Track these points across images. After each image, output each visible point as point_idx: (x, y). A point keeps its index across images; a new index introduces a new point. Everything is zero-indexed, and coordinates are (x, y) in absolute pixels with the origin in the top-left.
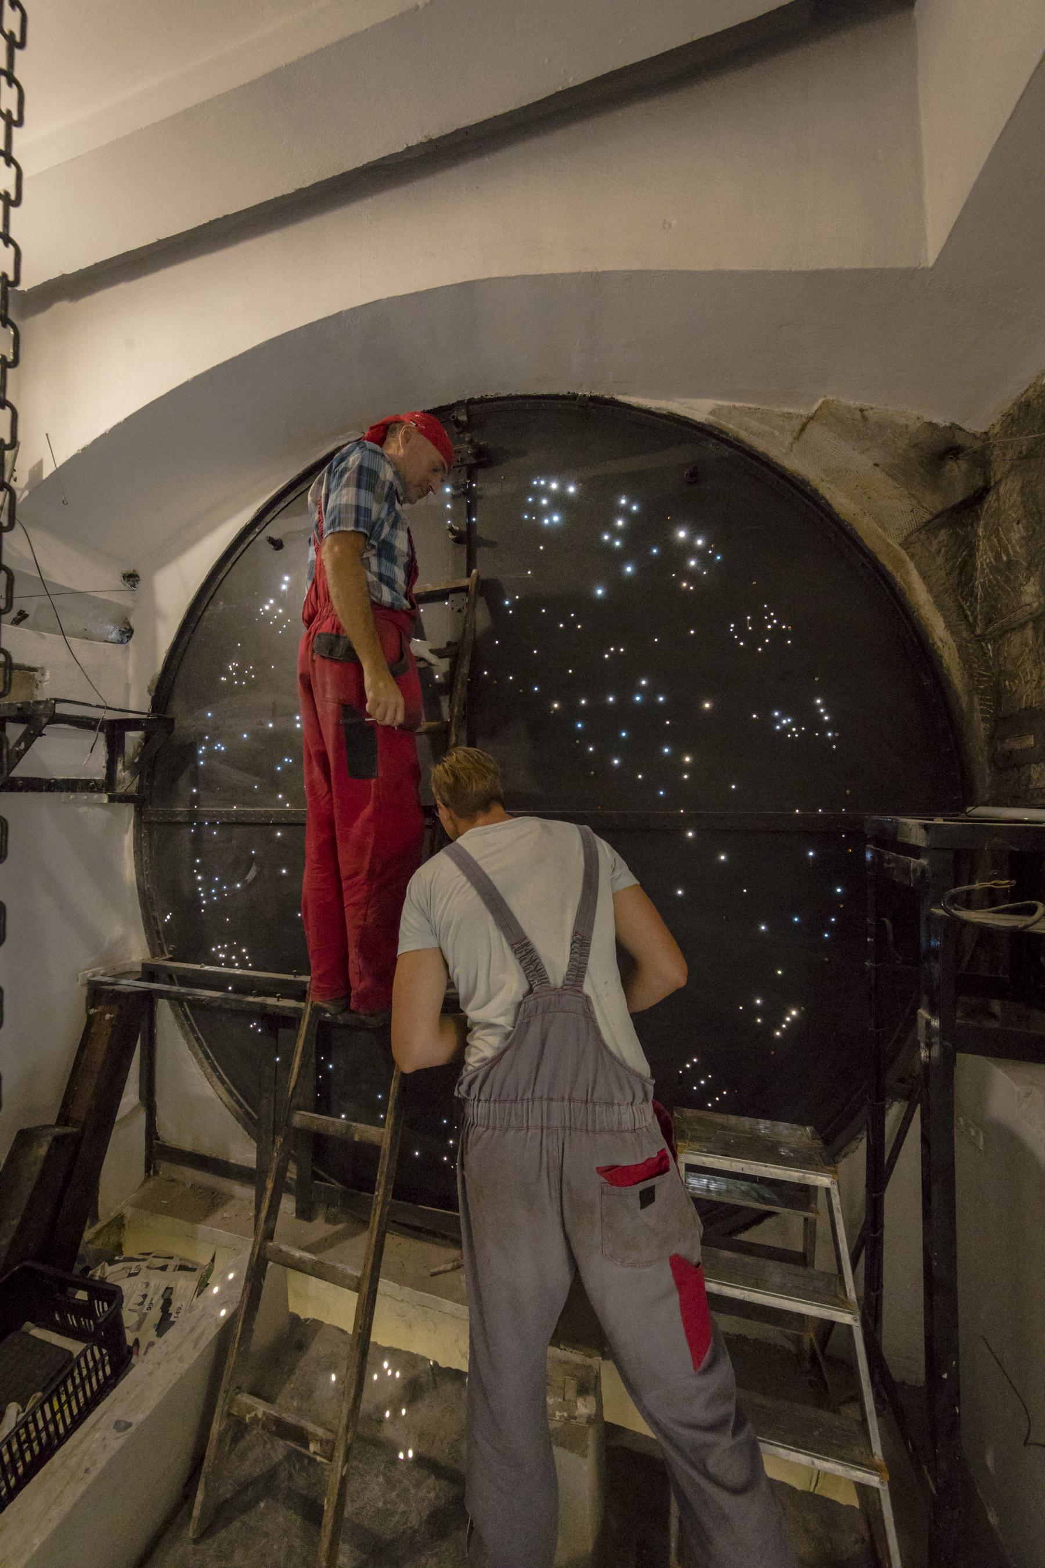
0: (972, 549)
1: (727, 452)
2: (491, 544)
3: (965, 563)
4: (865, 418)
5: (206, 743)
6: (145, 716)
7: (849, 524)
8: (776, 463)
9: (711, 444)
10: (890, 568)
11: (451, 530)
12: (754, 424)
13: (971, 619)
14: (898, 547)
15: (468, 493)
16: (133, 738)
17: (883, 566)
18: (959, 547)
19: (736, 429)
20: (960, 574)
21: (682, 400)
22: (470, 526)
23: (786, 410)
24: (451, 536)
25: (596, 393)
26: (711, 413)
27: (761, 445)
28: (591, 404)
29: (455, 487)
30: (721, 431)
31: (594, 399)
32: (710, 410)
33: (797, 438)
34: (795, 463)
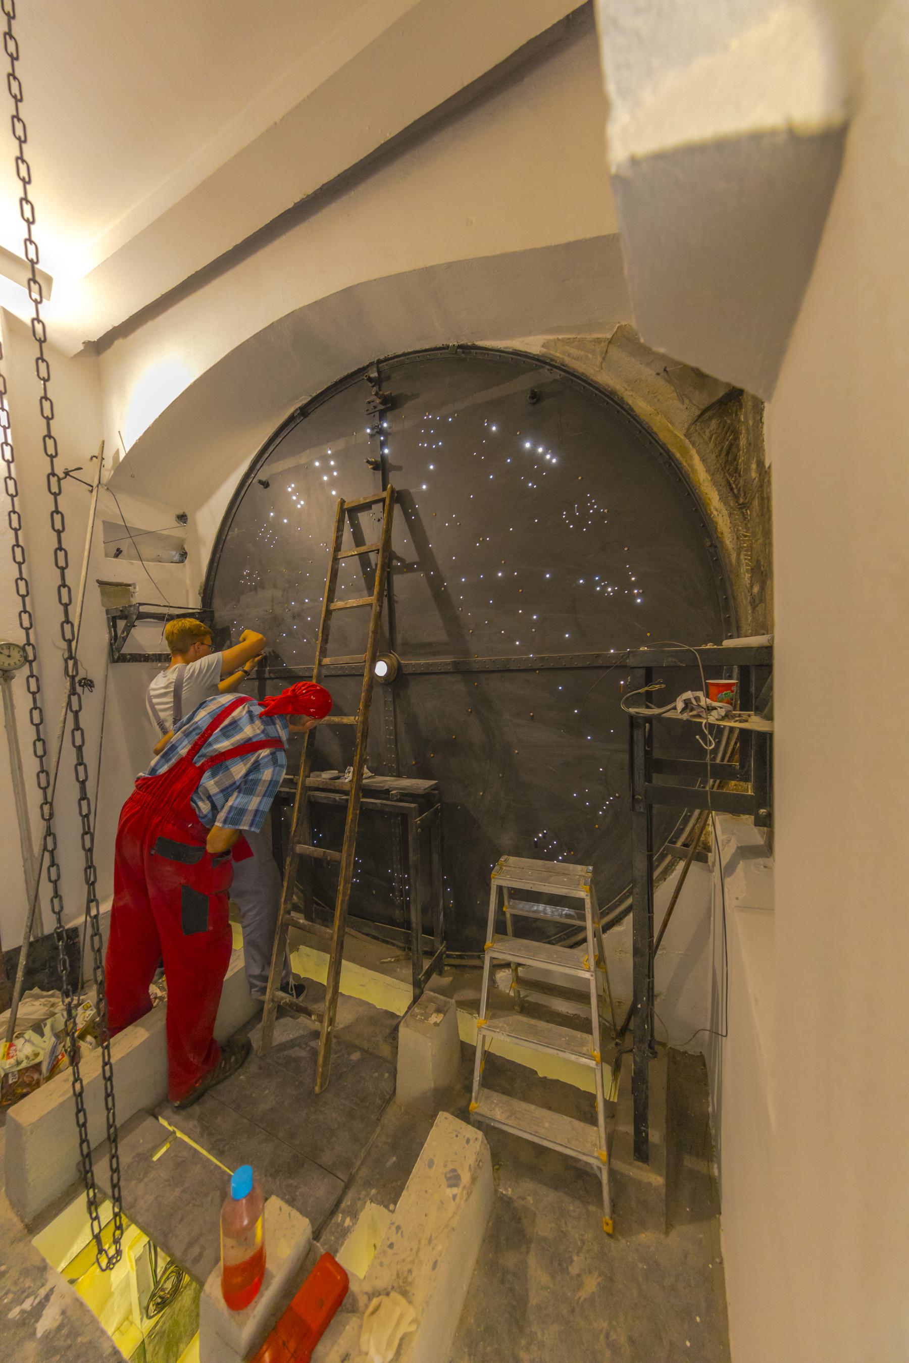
0: (736, 433)
2: (399, 468)
10: (678, 455)
14: (682, 437)
15: (381, 432)
17: (673, 454)
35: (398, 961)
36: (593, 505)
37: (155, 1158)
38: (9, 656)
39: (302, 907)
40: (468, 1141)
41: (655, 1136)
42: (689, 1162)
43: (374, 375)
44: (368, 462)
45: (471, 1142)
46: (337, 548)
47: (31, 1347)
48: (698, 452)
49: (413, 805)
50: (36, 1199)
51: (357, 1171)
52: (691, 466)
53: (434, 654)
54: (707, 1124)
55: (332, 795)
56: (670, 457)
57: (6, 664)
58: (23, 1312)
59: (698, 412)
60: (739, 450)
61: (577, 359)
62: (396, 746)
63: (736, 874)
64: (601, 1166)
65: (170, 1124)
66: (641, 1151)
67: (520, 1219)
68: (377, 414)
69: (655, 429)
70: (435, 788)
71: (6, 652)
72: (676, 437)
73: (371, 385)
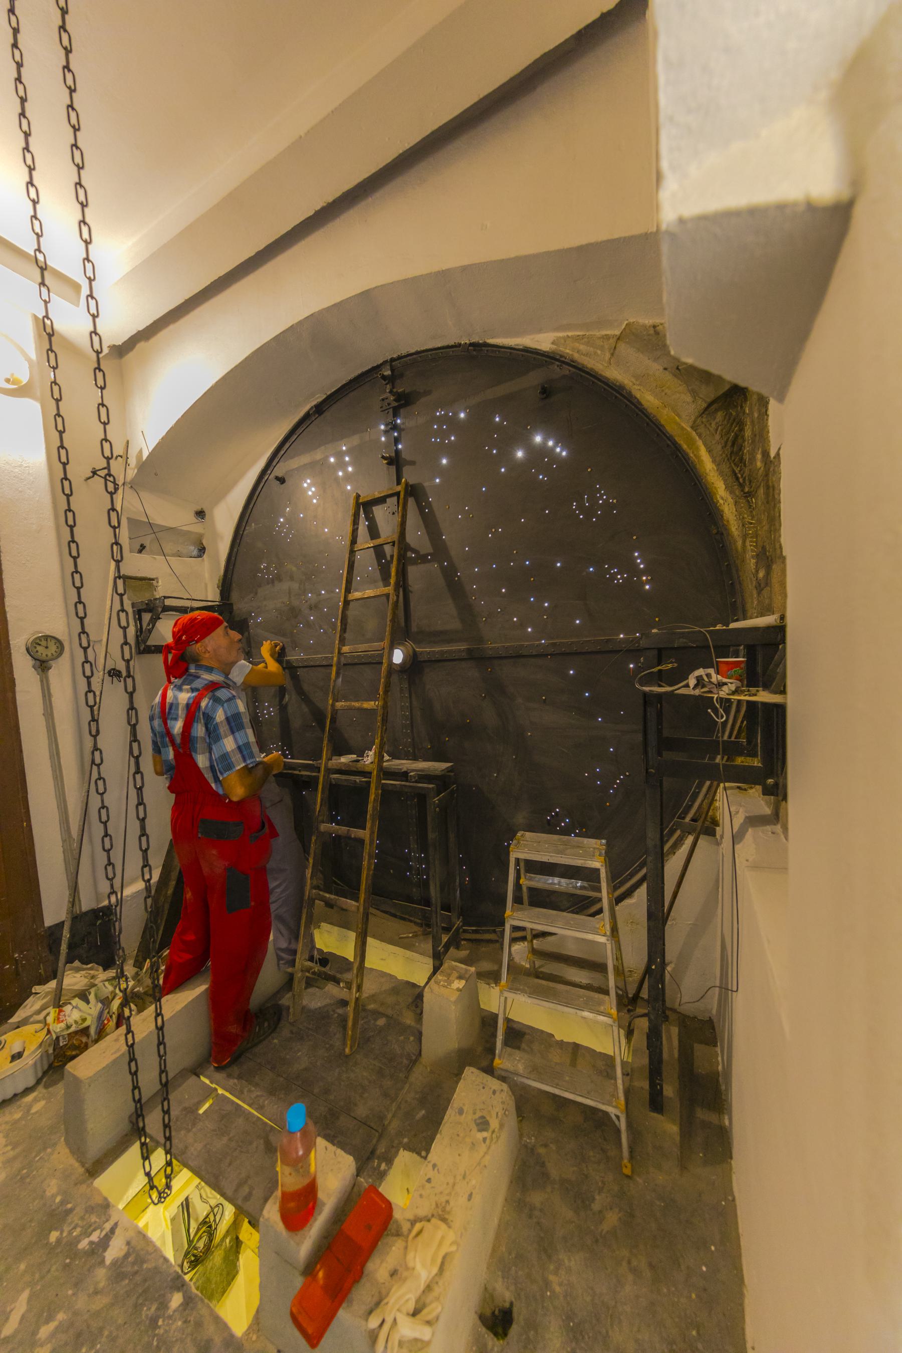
0: (741, 425)
2: (413, 463)
7: (654, 416)
8: (601, 375)
10: (685, 447)
14: (689, 429)
15: (395, 427)
20: (733, 445)
21: (532, 337)
23: (604, 332)
27: (590, 363)
29: (386, 425)
30: (561, 356)
32: (551, 341)
34: (614, 374)
35: (416, 936)
36: (602, 495)
37: (201, 1111)
38: (47, 647)
39: (322, 887)
40: (494, 1092)
41: (669, 1091)
42: (701, 1114)
43: (388, 373)
44: (383, 457)
45: (498, 1093)
46: (354, 541)
47: (101, 1274)
48: (705, 445)
49: (431, 786)
50: (95, 1146)
51: (390, 1123)
52: (698, 457)
53: (449, 641)
54: (718, 1081)
55: (352, 778)
56: (676, 448)
57: (44, 655)
58: (91, 1243)
59: (704, 405)
60: (744, 441)
61: (586, 355)
62: (412, 731)
63: (745, 840)
64: (619, 1114)
65: (211, 1083)
66: (656, 1103)
67: (543, 1163)
68: (391, 411)
69: (663, 422)
70: (449, 770)
71: (43, 643)
72: (683, 429)
73: (384, 383)
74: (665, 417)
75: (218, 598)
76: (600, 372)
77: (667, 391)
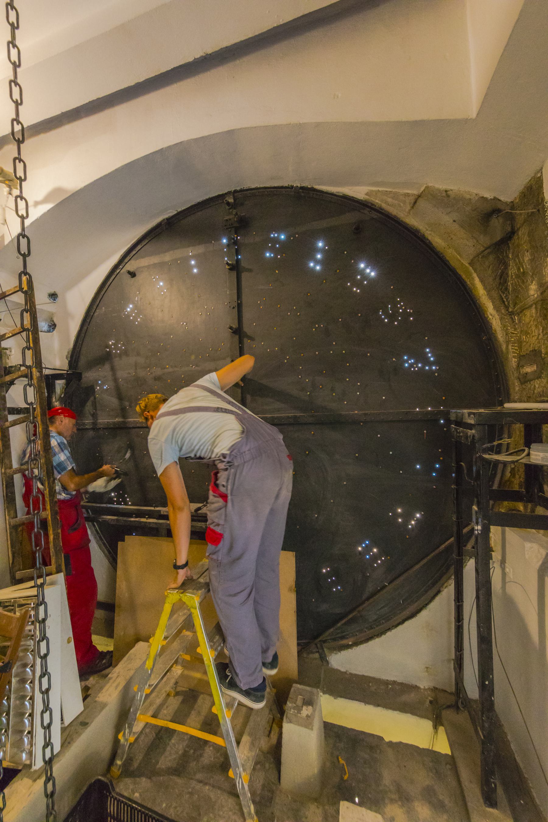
0: (506, 266)
1: (375, 215)
3: (502, 273)
4: (448, 196)
5: (99, 385)
6: (65, 372)
7: (441, 254)
9: (366, 211)
10: (464, 277)
11: (227, 264)
12: (390, 200)
13: (506, 303)
14: (467, 265)
16: (60, 384)
18: (499, 265)
19: (379, 202)
20: (501, 278)
21: (350, 188)
22: (238, 261)
24: (227, 267)
25: (303, 185)
26: (366, 194)
27: (393, 211)
28: (301, 190)
29: (229, 239)
30: (372, 204)
31: (302, 188)
33: (413, 207)
34: (412, 221)
52: (473, 285)
69: (447, 258)
74: (451, 255)
75: (66, 367)
76: (401, 219)
77: (452, 236)
